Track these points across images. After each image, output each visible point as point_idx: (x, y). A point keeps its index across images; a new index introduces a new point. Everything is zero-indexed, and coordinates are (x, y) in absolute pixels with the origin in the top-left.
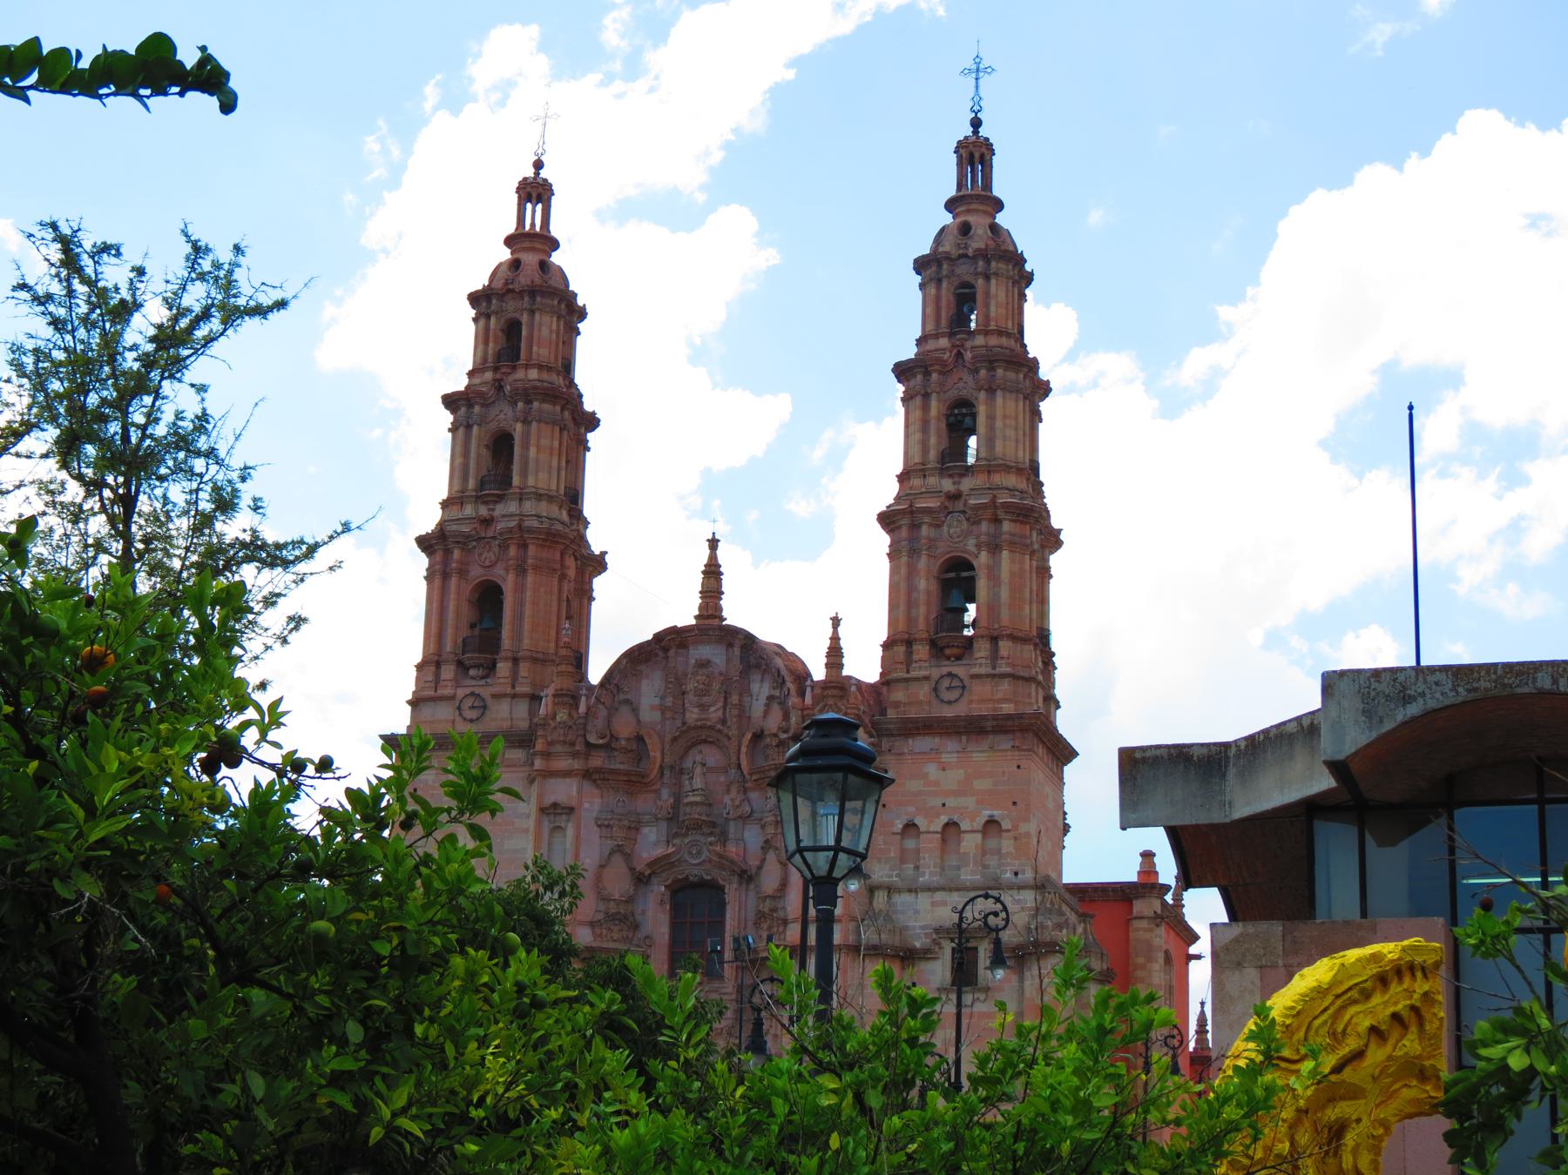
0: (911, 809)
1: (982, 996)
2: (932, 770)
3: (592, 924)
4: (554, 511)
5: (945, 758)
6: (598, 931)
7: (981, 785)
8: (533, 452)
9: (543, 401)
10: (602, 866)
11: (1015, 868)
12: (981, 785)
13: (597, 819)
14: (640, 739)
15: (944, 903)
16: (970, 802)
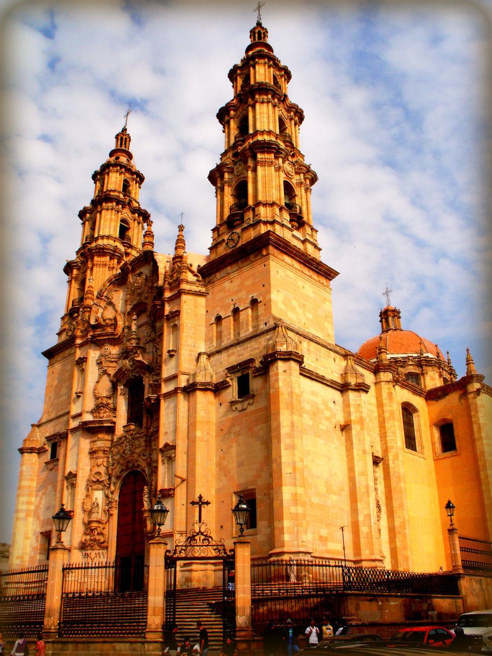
0: (219, 308)
1: (251, 401)
2: (227, 284)
3: (92, 412)
4: (111, 242)
5: (232, 276)
6: (95, 415)
7: (247, 283)
8: (102, 221)
9: (106, 202)
10: (97, 382)
11: (265, 321)
12: (247, 283)
13: (97, 360)
14: (115, 319)
15: (233, 354)
16: (243, 294)
